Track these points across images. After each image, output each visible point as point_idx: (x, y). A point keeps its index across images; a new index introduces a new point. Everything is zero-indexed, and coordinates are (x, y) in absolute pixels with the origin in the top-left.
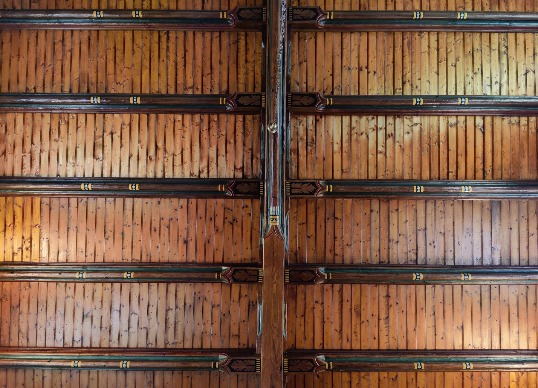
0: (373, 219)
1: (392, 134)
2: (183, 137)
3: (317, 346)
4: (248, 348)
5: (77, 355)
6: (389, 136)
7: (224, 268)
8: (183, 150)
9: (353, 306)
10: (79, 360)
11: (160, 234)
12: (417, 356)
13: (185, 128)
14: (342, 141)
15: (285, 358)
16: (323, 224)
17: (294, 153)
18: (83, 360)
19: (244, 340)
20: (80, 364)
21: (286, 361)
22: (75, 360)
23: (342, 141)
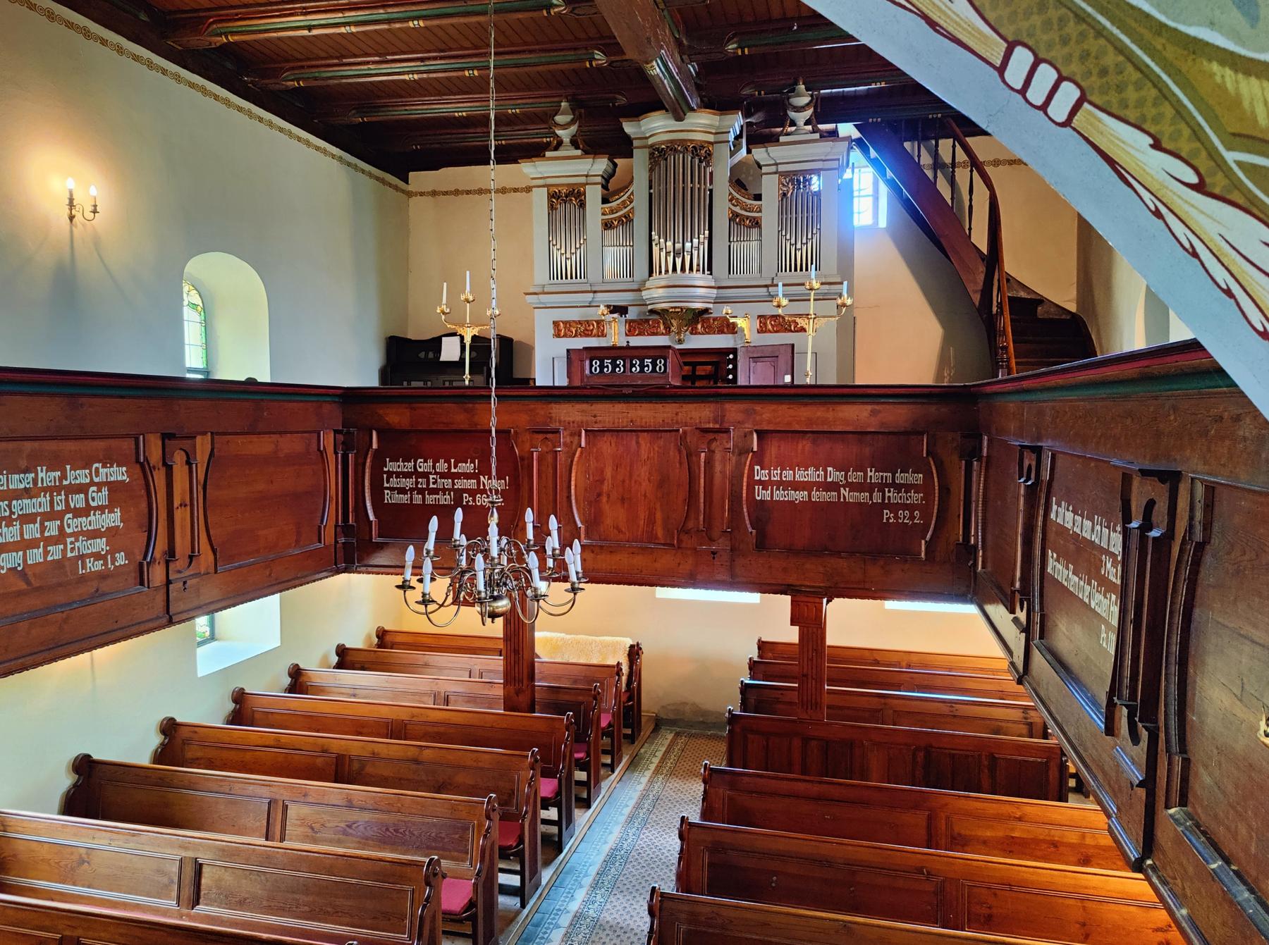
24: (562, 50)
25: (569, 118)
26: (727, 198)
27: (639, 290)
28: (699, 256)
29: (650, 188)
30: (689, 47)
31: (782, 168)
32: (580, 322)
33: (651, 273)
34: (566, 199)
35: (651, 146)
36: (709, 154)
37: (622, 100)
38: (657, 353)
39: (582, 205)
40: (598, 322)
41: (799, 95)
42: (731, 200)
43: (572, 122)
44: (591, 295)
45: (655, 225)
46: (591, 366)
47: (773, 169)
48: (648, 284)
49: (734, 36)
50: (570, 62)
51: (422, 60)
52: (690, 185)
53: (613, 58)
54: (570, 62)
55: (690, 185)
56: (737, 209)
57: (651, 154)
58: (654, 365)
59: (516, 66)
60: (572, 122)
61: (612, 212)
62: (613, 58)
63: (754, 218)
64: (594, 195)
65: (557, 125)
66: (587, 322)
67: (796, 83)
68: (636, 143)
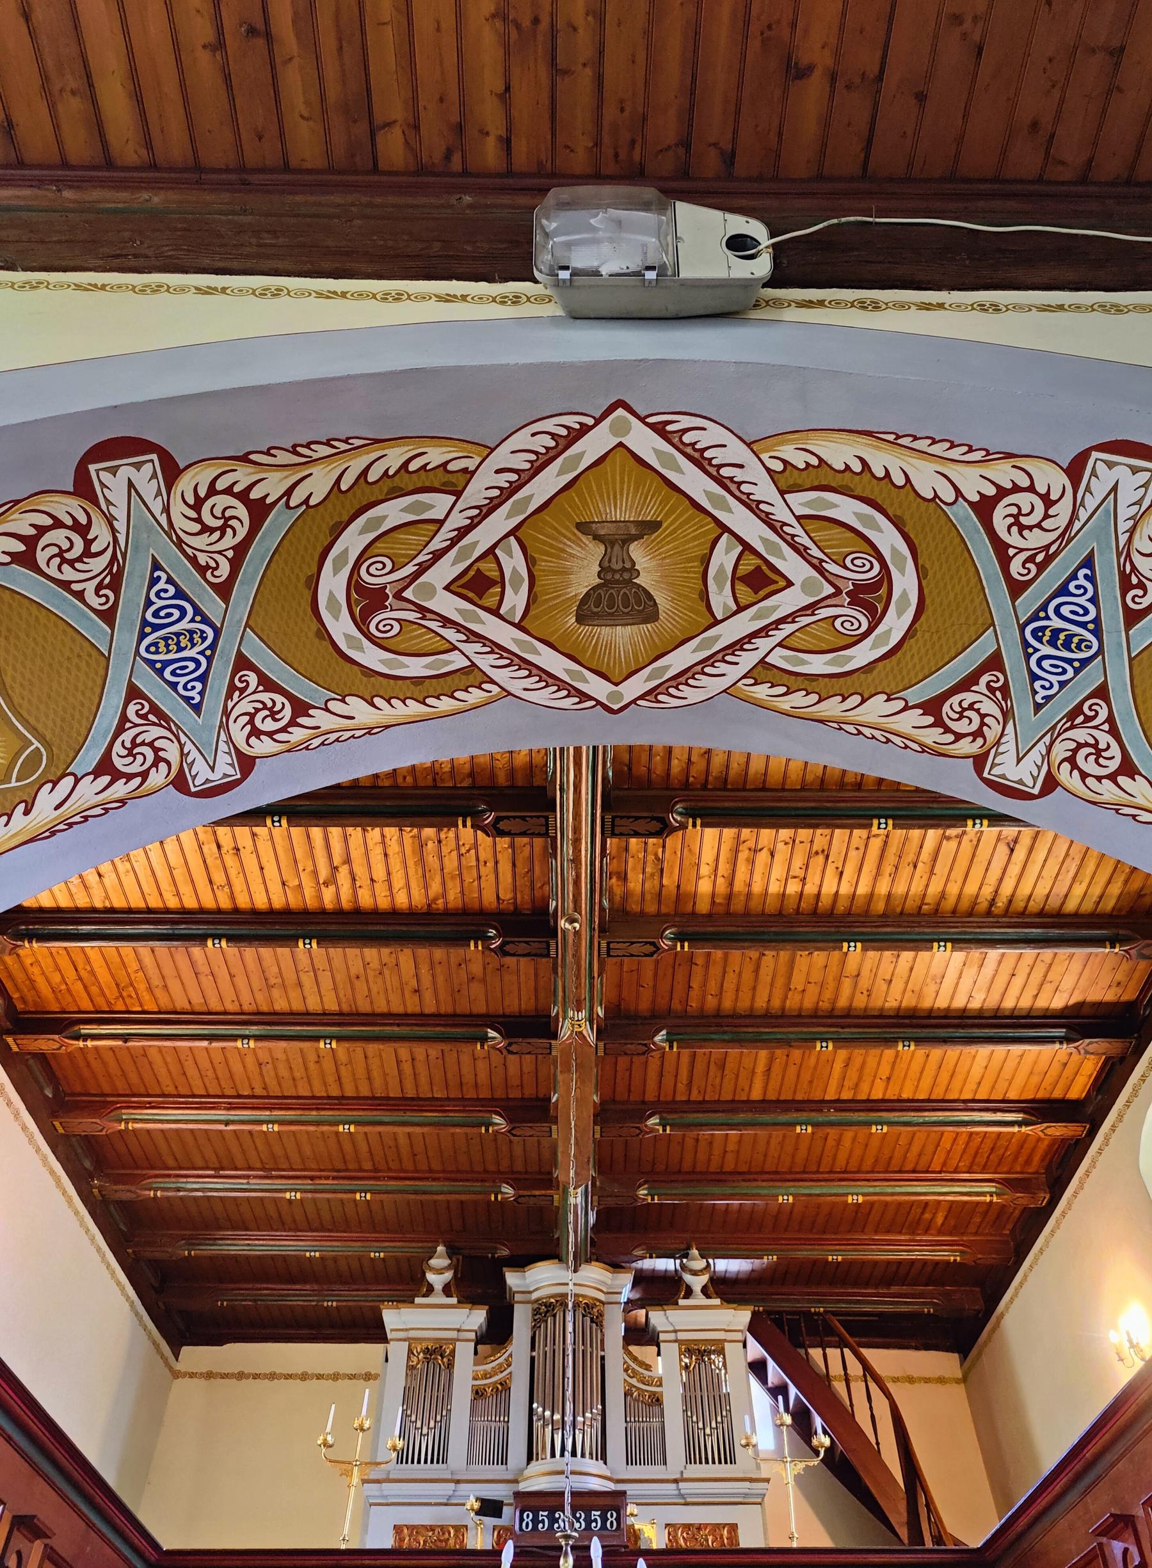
0: (763, 964)
1: (823, 851)
2: (386, 855)
3: (650, 1096)
4: (537, 1099)
5: (268, 1113)
6: (817, 853)
7: (492, 1033)
8: (389, 874)
9: (712, 1059)
10: (273, 1122)
11: (367, 981)
12: (805, 1114)
13: (387, 840)
14: (717, 860)
15: (595, 1123)
16: (671, 970)
17: (619, 878)
18: (281, 1123)
19: (529, 1092)
20: (276, 1128)
21: (598, 1128)
22: (268, 1122)
23: (717, 860)
24: (467, 1180)
25: (447, 1262)
26: (621, 1368)
27: (516, 1481)
28: (587, 1438)
29: (533, 1348)
30: (601, 1188)
31: (682, 1336)
32: (432, 1528)
33: (530, 1458)
34: (435, 1357)
35: (537, 1301)
36: (601, 1315)
37: (505, 1252)
38: (608, 1501)
39: (450, 1366)
40: (457, 1528)
41: (694, 1259)
42: (626, 1370)
43: (448, 1268)
44: (452, 1486)
45: (539, 1394)
46: (522, 1520)
47: (672, 1336)
48: (527, 1473)
49: (646, 1182)
50: (474, 1193)
51: (312, 1178)
52: (582, 1348)
53: (521, 1192)
54: (474, 1193)
55: (582, 1348)
56: (634, 1381)
57: (536, 1312)
58: (604, 1520)
59: (416, 1193)
60: (448, 1268)
61: (486, 1376)
62: (521, 1192)
63: (654, 1393)
64: (464, 1353)
65: (431, 1269)
66: (442, 1527)
67: (689, 1248)
68: (518, 1297)
